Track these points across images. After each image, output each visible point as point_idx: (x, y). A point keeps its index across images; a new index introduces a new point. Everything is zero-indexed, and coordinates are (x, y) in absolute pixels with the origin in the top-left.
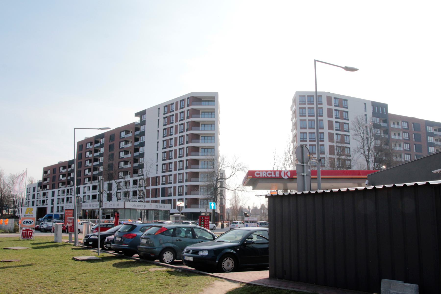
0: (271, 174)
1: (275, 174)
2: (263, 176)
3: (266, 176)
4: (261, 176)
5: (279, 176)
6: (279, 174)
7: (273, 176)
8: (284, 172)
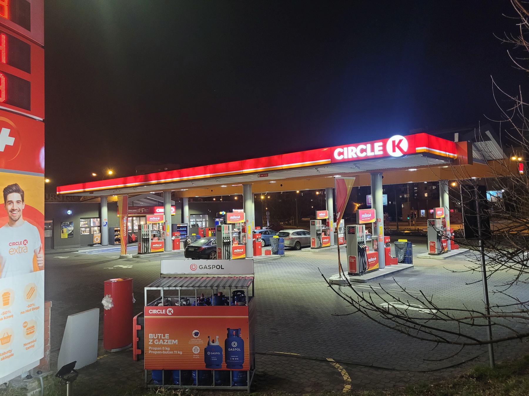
0: (160, 312)
1: (162, 312)
2: (154, 313)
3: (156, 313)
4: (153, 313)
5: (165, 313)
6: (165, 312)
7: (161, 313)
8: (169, 310)
